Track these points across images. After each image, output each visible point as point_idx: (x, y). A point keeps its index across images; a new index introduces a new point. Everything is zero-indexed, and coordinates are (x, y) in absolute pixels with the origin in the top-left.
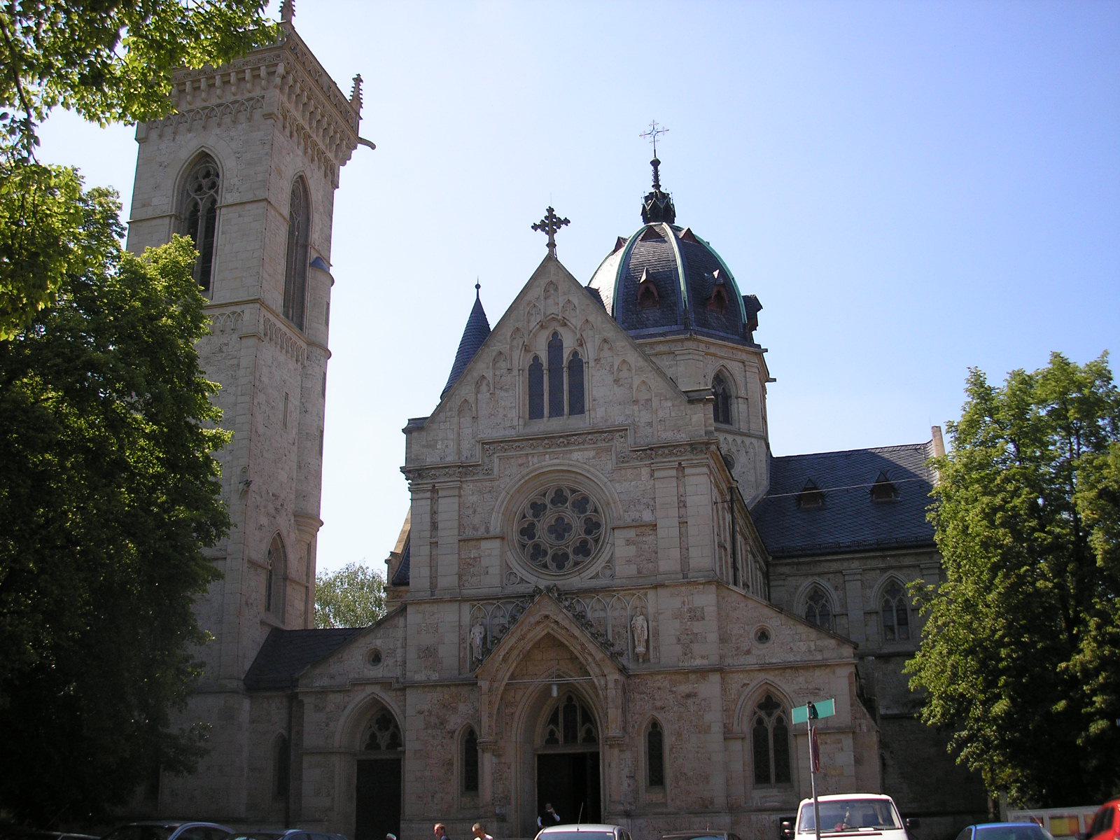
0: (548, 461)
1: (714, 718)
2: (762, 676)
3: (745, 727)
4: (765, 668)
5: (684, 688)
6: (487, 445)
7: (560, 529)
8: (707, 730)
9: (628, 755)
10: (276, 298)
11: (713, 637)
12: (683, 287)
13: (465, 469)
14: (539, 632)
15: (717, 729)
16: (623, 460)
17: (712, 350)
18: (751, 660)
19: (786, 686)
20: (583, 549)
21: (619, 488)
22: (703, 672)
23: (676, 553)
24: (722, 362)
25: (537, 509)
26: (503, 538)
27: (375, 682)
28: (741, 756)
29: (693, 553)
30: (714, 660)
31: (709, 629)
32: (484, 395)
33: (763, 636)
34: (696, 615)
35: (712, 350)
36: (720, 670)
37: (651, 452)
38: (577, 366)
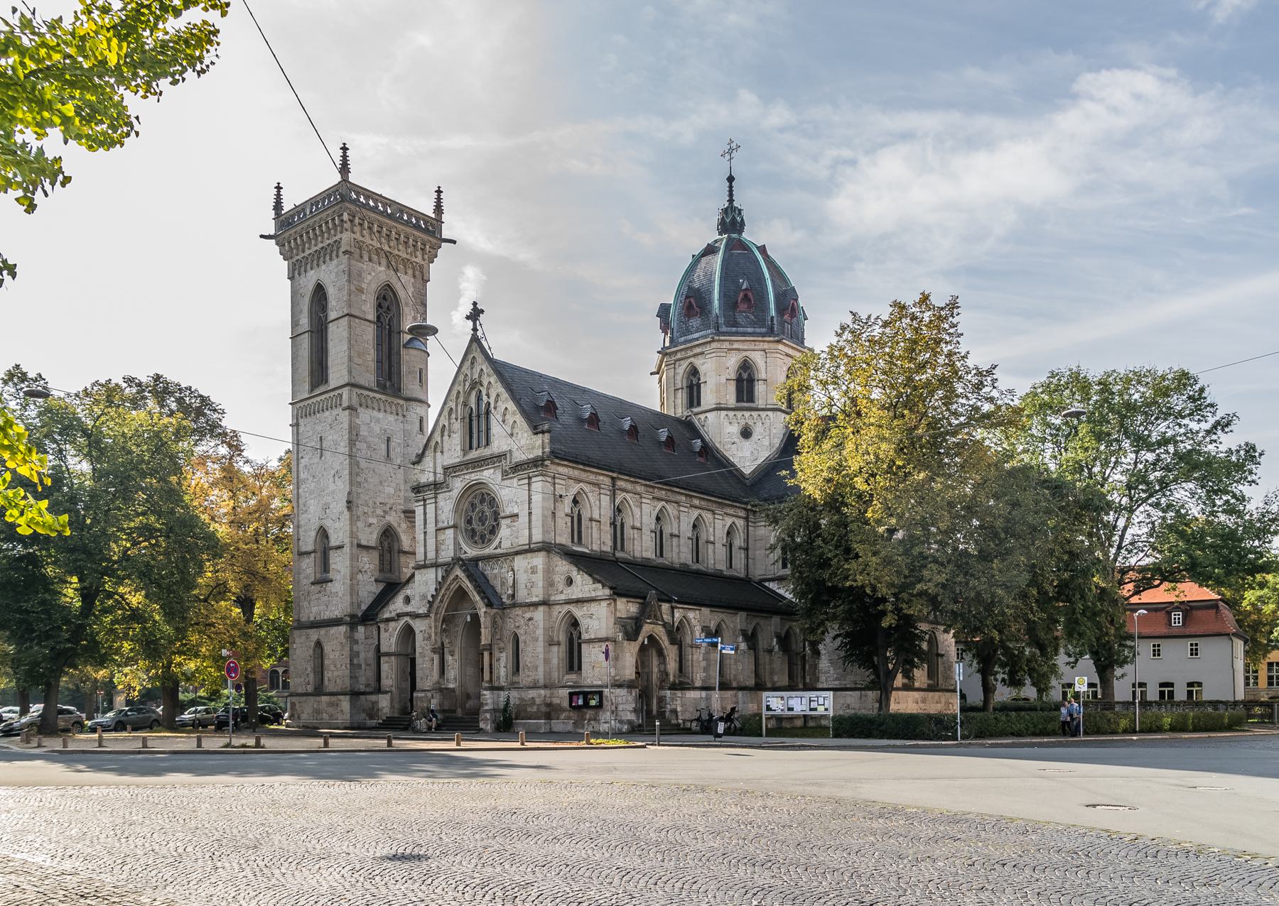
0: (474, 477)
1: (540, 632)
2: (567, 608)
3: (562, 638)
4: (569, 602)
5: (528, 615)
6: (446, 469)
7: (482, 520)
8: (537, 640)
9: (504, 654)
10: (369, 379)
11: (541, 584)
12: (716, 303)
13: (436, 486)
14: (454, 587)
15: (541, 638)
16: (505, 475)
17: (736, 346)
18: (563, 597)
19: (578, 612)
20: (493, 531)
21: (510, 494)
22: (535, 605)
23: (527, 532)
24: (745, 354)
25: (473, 505)
26: (455, 526)
27: (407, 614)
28: (558, 655)
29: (534, 531)
30: (541, 598)
31: (539, 579)
32: (446, 438)
33: (570, 582)
34: (534, 570)
35: (736, 346)
36: (545, 603)
37: (518, 468)
38: (488, 413)
